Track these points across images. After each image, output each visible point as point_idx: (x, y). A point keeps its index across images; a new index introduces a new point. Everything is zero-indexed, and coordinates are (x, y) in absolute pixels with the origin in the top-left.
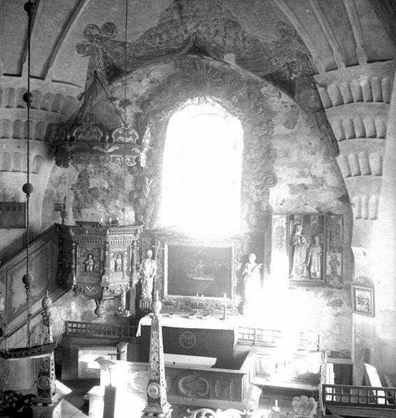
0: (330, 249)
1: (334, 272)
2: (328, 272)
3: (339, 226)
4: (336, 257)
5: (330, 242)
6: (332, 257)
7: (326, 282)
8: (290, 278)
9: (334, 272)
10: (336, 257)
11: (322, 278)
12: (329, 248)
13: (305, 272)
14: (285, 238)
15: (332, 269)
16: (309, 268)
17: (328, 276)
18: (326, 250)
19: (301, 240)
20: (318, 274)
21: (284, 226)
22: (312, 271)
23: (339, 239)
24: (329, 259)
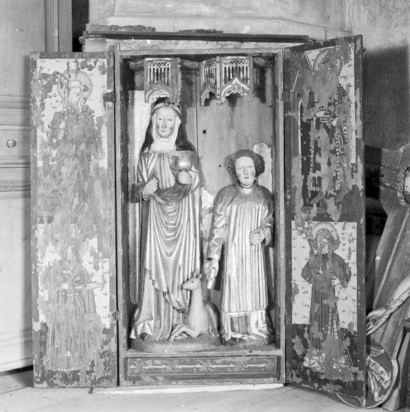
0: (307, 205)
1: (323, 311)
2: (301, 313)
3: (342, 93)
4: (334, 242)
5: (305, 171)
6: (312, 242)
7: (294, 360)
8: (130, 344)
9: (323, 311)
10: (334, 242)
11: (273, 340)
12: (299, 202)
13: (200, 318)
14: (104, 163)
15: (317, 297)
16: (214, 303)
17: (298, 330)
18: (290, 216)
19: (175, 169)
20: (258, 322)
21: (99, 109)
22: (231, 310)
23: (345, 154)
24: (301, 253)
